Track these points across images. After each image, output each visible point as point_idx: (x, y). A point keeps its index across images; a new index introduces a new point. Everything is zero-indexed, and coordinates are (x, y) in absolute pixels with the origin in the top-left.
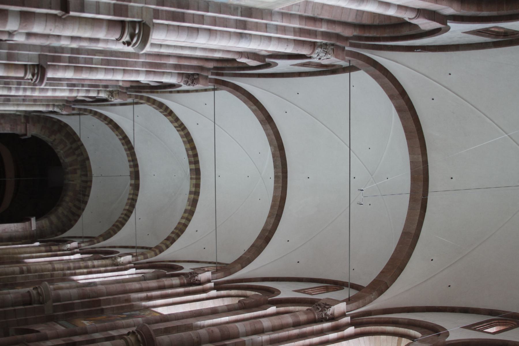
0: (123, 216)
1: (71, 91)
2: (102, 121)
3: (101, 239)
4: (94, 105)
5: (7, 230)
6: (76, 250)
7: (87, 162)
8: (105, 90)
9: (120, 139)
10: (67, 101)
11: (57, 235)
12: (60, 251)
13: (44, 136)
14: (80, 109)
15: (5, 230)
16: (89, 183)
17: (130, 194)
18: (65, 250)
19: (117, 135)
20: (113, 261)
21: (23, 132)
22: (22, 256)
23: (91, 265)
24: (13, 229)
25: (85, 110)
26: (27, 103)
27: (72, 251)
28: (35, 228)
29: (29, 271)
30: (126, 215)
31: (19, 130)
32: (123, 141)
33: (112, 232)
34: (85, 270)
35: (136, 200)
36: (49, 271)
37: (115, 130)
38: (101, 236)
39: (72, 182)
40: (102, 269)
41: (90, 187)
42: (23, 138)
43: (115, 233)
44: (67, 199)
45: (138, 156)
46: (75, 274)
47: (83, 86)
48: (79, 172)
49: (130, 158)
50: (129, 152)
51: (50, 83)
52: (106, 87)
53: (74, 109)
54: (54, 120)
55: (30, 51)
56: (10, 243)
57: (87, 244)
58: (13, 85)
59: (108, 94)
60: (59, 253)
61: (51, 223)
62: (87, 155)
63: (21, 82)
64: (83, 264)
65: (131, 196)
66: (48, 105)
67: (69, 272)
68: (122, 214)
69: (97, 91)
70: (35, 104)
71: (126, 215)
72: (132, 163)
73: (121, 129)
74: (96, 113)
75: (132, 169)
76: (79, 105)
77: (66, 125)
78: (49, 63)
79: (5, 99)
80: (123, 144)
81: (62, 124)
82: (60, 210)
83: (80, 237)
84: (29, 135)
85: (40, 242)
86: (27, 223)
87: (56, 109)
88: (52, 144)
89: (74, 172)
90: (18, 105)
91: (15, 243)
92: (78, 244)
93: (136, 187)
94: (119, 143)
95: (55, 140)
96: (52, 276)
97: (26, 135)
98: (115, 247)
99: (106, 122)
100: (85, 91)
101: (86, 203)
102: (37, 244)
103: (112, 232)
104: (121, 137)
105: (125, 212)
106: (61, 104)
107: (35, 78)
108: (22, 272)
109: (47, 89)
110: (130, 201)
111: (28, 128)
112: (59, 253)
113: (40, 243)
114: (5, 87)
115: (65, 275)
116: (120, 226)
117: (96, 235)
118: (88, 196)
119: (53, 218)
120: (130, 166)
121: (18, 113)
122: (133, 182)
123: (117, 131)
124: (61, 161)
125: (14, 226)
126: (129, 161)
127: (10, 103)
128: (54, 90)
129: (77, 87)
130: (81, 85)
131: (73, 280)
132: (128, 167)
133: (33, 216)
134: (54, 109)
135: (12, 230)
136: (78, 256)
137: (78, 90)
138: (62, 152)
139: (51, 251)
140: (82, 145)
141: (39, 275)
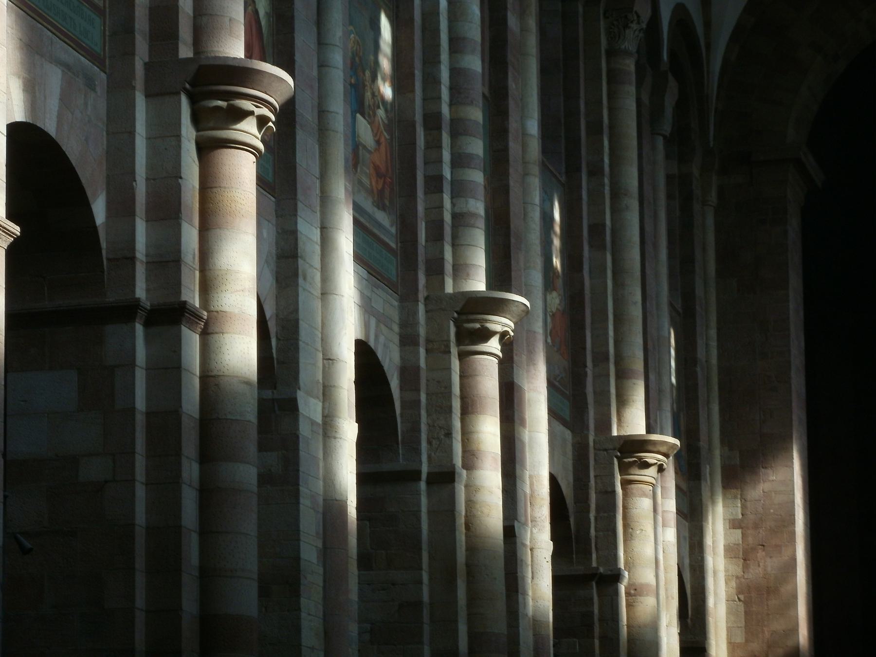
26: (606, 160)
55: (132, 133)
58: (441, 207)
63: (428, 179)
70: (611, 127)
78: (185, 52)
79: (591, 246)
87: (631, 41)
90: (616, 195)
107: (247, 105)
114: (455, 237)
121: (713, 197)
127: (608, 223)
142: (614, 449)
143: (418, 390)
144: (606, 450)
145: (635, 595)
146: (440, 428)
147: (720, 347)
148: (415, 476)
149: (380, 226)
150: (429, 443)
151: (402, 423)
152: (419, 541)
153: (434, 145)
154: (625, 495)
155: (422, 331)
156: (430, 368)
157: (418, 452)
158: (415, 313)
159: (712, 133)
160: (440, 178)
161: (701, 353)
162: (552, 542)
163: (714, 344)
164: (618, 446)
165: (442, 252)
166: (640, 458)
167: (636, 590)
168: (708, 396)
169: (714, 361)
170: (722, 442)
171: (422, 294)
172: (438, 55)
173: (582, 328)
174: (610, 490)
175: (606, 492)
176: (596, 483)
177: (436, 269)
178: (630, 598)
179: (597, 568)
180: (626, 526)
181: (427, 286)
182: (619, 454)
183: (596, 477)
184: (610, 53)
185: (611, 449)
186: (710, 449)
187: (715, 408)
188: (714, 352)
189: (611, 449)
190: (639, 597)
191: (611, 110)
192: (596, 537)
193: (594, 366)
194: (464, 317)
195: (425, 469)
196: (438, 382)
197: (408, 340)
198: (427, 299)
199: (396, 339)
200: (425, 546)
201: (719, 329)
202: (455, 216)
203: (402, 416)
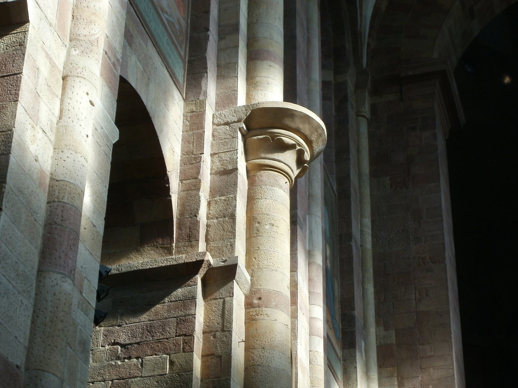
121: (366, 110)
142: (239, 121)
147: (374, 236)
162: (118, 130)
163: (368, 231)
167: (260, 299)
168: (363, 277)
169: (369, 245)
170: (377, 323)
178: (252, 309)
179: (204, 254)
185: (235, 122)
186: (365, 326)
187: (370, 289)
189: (235, 122)
190: (264, 309)
192: (208, 226)
201: (373, 222)
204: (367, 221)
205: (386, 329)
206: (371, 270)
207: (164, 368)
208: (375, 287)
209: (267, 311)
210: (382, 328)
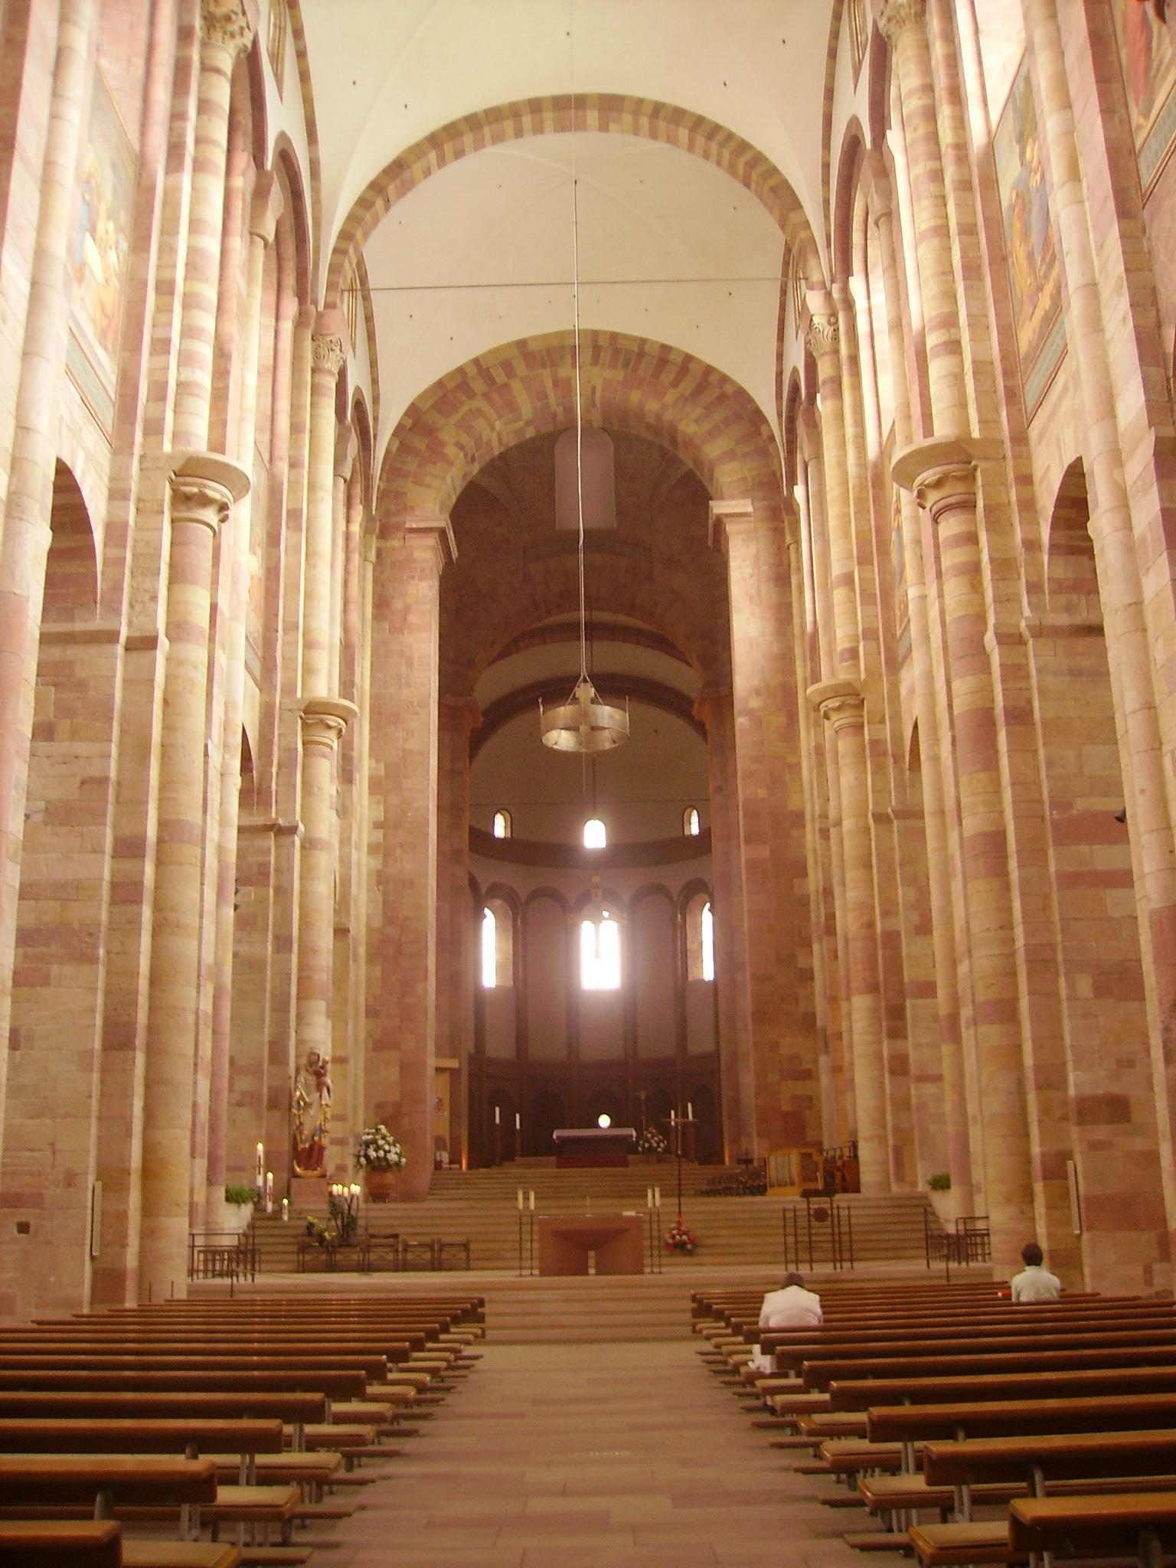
0: (714, 146)
1: (199, 166)
2: (376, 221)
3: (794, 217)
4: (317, 239)
5: (753, 592)
6: (836, 295)
7: (532, 347)
8: (205, 45)
9: (442, 162)
10: (300, 323)
11: (772, 438)
12: (836, 352)
13: (449, 479)
14: (331, 286)
15: (751, 598)
16: (602, 341)
17: (636, 132)
18: (836, 330)
19: (427, 173)
20: (901, 22)
21: (432, 541)
22: (852, 469)
23: (920, 98)
24: (747, 571)
25: (335, 269)
27: (839, 306)
28: (749, 501)
29: (949, 321)
30: (710, 137)
31: (426, 555)
32: (448, 148)
33: (772, 182)
34: (945, 112)
35: (658, 109)
36: (948, 249)
37: (406, 174)
38: (783, 224)
39: (598, 394)
40: (938, 50)
41: (614, 336)
42: (455, 554)
43: (774, 171)
44: (652, 406)
45: (500, 98)
46: (961, 148)
47: (177, 116)
48: (563, 372)
49: (509, 125)
50: (487, 130)
51: (162, 232)
52: (184, 34)
53: (330, 306)
54: (394, 449)
56: (794, 580)
57: (812, 263)
59: (218, 35)
60: (844, 351)
61: (731, 455)
62: (509, 345)
64: (915, 130)
65: (645, 121)
66: (315, 390)
67: (950, 174)
68: (706, 156)
69: (207, 74)
71: (710, 137)
72: (527, 120)
73: (402, 153)
74: (345, 235)
75: (548, 116)
76: (315, 289)
77: (413, 410)
79: (288, 527)
80: (459, 154)
81: (409, 422)
82: (689, 427)
83: (780, 357)
84: (442, 521)
85: (792, 481)
86: (730, 528)
88: (473, 459)
89: (564, 387)
90: (312, 487)
91: (793, 564)
92: (812, 289)
93: (611, 106)
94: (455, 169)
95: (460, 446)
96: (968, 230)
97: (442, 533)
98: (826, 166)
99: (379, 203)
100: (204, 118)
101: (666, 349)
102: (799, 492)
103: (772, 182)
104: (433, 156)
105: (700, 140)
106: (308, 345)
108: (953, 347)
109: (193, 251)
110: (662, 125)
111: (421, 525)
112: (844, 351)
113: (797, 484)
114: (176, 405)
115: (964, 185)
116: (748, 156)
117: (777, 240)
118: (643, 341)
119: (713, 450)
120: (538, 130)
121: (372, 555)
122: (592, 116)
123: (409, 166)
124: (530, 433)
125: (739, 567)
126: (519, 133)
128: (195, 226)
129: (182, 135)
130: (177, 124)
131: (990, 148)
132: (539, 137)
133: (707, 508)
134: (330, 372)
135: (751, 576)
136: (856, 284)
137: (198, 141)
138: (498, 425)
139: (837, 381)
140: (476, 362)
141: (965, 278)
143: (123, 546)
144: (290, 710)
145: (310, 849)
146: (145, 591)
147: (373, 677)
148: (112, 637)
149: (99, 362)
150: (132, 606)
151: (102, 581)
152: (112, 710)
153: (165, 309)
154: (305, 754)
155: (134, 486)
156: (138, 528)
157: (118, 612)
158: (128, 467)
159: (374, 505)
160: (167, 342)
161: (357, 679)
163: (367, 673)
164: (302, 707)
165: (163, 412)
166: (322, 721)
169: (367, 688)
170: (370, 756)
171: (137, 450)
172: (177, 226)
173: (277, 597)
174: (292, 747)
175: (289, 750)
176: (280, 740)
177: (154, 428)
179: (277, 819)
180: (306, 783)
181: (143, 446)
182: (303, 714)
183: (279, 735)
184: (314, 371)
186: (360, 760)
188: (368, 680)
191: (311, 416)
192: (277, 791)
193: (285, 633)
194: (181, 480)
195: (124, 633)
196: (148, 543)
197: (117, 494)
198: (142, 458)
199: (105, 492)
200: (116, 716)
201: (372, 663)
202: (180, 385)
203: (103, 573)
204: (367, 664)
205: (376, 762)
206: (368, 710)
207: (250, 895)
208: (370, 724)
209: (316, 852)
210: (374, 761)
